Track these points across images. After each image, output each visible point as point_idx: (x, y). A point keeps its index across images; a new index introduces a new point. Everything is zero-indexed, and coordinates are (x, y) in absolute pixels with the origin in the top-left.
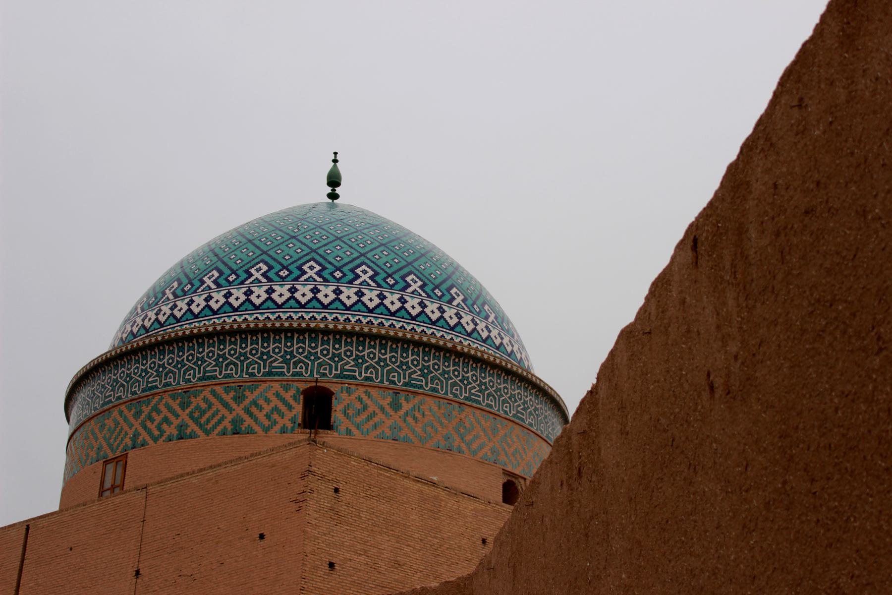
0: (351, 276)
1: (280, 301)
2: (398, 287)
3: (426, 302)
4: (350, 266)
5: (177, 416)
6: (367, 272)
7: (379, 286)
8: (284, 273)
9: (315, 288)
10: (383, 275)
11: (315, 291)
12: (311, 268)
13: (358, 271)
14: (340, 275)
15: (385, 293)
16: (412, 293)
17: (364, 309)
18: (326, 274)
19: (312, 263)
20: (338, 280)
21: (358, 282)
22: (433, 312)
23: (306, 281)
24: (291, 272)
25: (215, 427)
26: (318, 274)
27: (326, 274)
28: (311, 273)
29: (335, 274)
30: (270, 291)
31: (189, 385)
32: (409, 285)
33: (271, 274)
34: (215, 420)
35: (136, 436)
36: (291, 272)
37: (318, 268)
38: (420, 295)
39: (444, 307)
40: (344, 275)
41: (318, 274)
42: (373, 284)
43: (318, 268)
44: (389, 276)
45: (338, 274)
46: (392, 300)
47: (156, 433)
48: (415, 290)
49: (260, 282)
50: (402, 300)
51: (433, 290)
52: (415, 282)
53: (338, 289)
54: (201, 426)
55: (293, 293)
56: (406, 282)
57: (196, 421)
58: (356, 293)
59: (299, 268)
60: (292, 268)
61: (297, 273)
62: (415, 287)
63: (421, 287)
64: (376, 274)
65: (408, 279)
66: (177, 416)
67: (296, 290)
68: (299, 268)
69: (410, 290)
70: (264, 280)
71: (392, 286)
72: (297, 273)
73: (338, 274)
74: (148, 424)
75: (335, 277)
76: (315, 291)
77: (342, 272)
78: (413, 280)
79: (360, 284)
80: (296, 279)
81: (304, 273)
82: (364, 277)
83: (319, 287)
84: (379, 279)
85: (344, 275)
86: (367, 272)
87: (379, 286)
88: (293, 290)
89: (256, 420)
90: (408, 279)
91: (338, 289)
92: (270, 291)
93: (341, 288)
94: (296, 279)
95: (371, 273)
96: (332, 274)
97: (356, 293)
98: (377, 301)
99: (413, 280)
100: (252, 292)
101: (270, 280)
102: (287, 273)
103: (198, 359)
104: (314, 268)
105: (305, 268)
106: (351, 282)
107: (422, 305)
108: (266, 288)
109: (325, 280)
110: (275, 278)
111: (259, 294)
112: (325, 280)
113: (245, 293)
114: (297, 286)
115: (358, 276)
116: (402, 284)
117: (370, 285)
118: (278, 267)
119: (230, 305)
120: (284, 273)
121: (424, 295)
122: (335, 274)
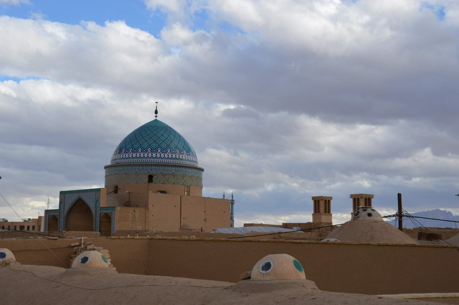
0: (166, 151)
2: (175, 153)
4: (166, 149)
5: (182, 180)
7: (171, 153)
8: (154, 151)
12: (159, 150)
18: (152, 151)
19: (159, 148)
24: (156, 151)
25: (170, 183)
26: (161, 151)
30: (152, 155)
31: (157, 174)
33: (152, 151)
34: (170, 181)
35: (191, 184)
36: (156, 151)
37: (160, 150)
41: (161, 151)
42: (170, 153)
46: (174, 156)
47: (179, 183)
54: (168, 182)
57: (167, 181)
60: (156, 149)
61: (157, 151)
66: (163, 179)
68: (157, 149)
71: (174, 153)
72: (157, 151)
73: (164, 151)
74: (176, 180)
80: (157, 152)
81: (158, 151)
84: (171, 152)
87: (171, 153)
88: (156, 155)
89: (157, 181)
92: (152, 155)
96: (163, 151)
101: (152, 152)
106: (166, 153)
107: (179, 156)
112: (162, 152)
114: (157, 154)
115: (168, 151)
118: (153, 149)
119: (149, 157)
120: (154, 151)
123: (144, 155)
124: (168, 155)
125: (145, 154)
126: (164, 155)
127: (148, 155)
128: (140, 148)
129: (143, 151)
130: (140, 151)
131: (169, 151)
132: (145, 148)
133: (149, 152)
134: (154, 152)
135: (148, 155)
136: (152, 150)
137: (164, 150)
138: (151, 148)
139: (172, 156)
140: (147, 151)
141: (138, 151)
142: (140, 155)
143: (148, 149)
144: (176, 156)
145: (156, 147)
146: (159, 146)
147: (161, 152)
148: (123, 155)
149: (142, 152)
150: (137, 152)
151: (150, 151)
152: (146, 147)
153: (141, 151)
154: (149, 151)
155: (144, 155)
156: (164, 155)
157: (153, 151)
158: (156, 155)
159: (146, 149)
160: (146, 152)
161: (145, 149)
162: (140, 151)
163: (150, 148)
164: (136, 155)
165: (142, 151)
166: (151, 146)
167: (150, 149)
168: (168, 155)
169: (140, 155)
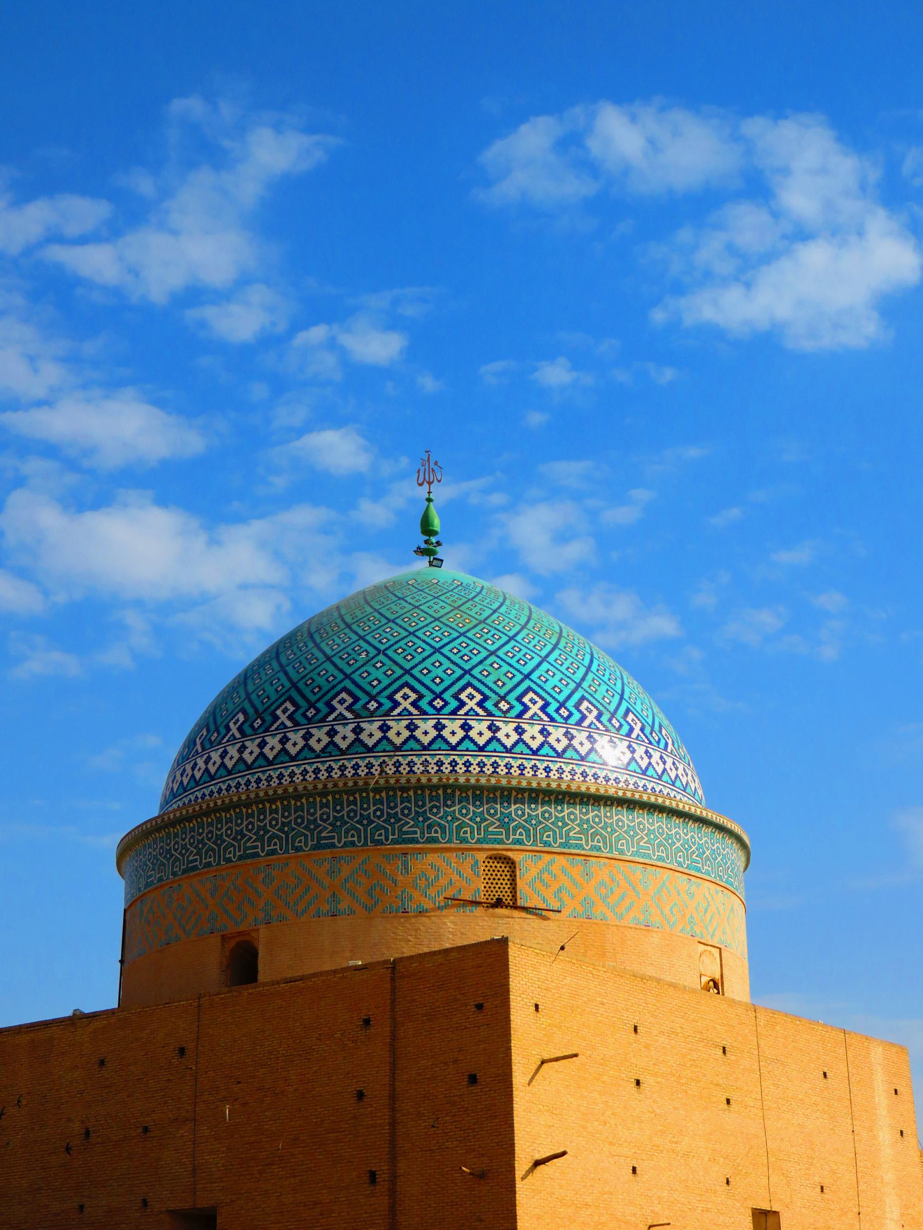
0: (454, 704)
1: (370, 742)
3: (549, 728)
6: (473, 697)
9: (411, 723)
10: (495, 698)
11: (412, 727)
12: (405, 697)
13: (463, 696)
14: (442, 703)
15: (498, 724)
16: (531, 718)
17: (472, 747)
19: (406, 690)
20: (439, 710)
21: (462, 712)
22: (558, 740)
23: (399, 715)
26: (414, 704)
27: (423, 704)
28: (406, 704)
29: (435, 703)
30: (358, 730)
32: (526, 709)
36: (380, 705)
37: (413, 696)
38: (541, 720)
39: (572, 731)
40: (446, 703)
41: (414, 704)
43: (413, 696)
44: (503, 698)
45: (438, 703)
48: (535, 714)
49: (346, 719)
50: (519, 730)
51: (557, 710)
52: (535, 703)
53: (439, 723)
55: (384, 732)
56: (523, 704)
58: (462, 727)
59: (391, 698)
62: (534, 709)
63: (543, 709)
64: (485, 698)
65: (526, 700)
67: (389, 728)
68: (391, 698)
69: (527, 716)
70: (348, 715)
71: (505, 713)
72: (388, 704)
75: (434, 708)
76: (412, 727)
77: (443, 700)
78: (531, 700)
79: (466, 714)
80: (387, 714)
81: (396, 704)
82: (471, 704)
83: (416, 722)
84: (489, 705)
85: (446, 703)
86: (473, 697)
87: (490, 714)
88: (384, 728)
90: (526, 700)
91: (439, 723)
92: (358, 730)
93: (443, 722)
94: (387, 714)
95: (479, 697)
97: (462, 727)
98: (488, 734)
99: (531, 700)
100: (336, 733)
101: (357, 716)
102: (376, 705)
103: (283, 824)
104: (409, 697)
105: (398, 697)
108: (352, 726)
109: (425, 713)
110: (364, 713)
111: (345, 733)
113: (304, 737)
114: (390, 723)
115: (462, 704)
116: (519, 708)
117: (477, 715)
118: (364, 698)
120: (373, 705)
121: (545, 718)
122: (435, 703)
123: (307, 736)
124: (466, 727)
125: (313, 731)
126: (439, 727)
127: (332, 733)
128: (288, 704)
129: (304, 715)
130: (283, 718)
131: (471, 704)
132: (313, 698)
133: (341, 717)
134: (372, 714)
135: (332, 733)
136: (361, 703)
137: (439, 696)
138: (351, 694)
139: (493, 728)
140: (324, 710)
141: (276, 718)
142: (284, 740)
143: (335, 703)
144: (519, 730)
145: (386, 682)
146: (407, 678)
147: (415, 712)
148: (241, 750)
149: (296, 724)
150: (267, 730)
151: (349, 709)
152: (325, 689)
153: (290, 718)
154: (341, 709)
155: (307, 736)
156: (439, 727)
157: (365, 707)
158: (384, 728)
159: (320, 705)
160: (323, 720)
161: (312, 705)
162: (283, 718)
163: (344, 695)
164: (262, 744)
165: (298, 717)
166: (354, 682)
167: (350, 700)
168: (466, 727)
169: (284, 740)
